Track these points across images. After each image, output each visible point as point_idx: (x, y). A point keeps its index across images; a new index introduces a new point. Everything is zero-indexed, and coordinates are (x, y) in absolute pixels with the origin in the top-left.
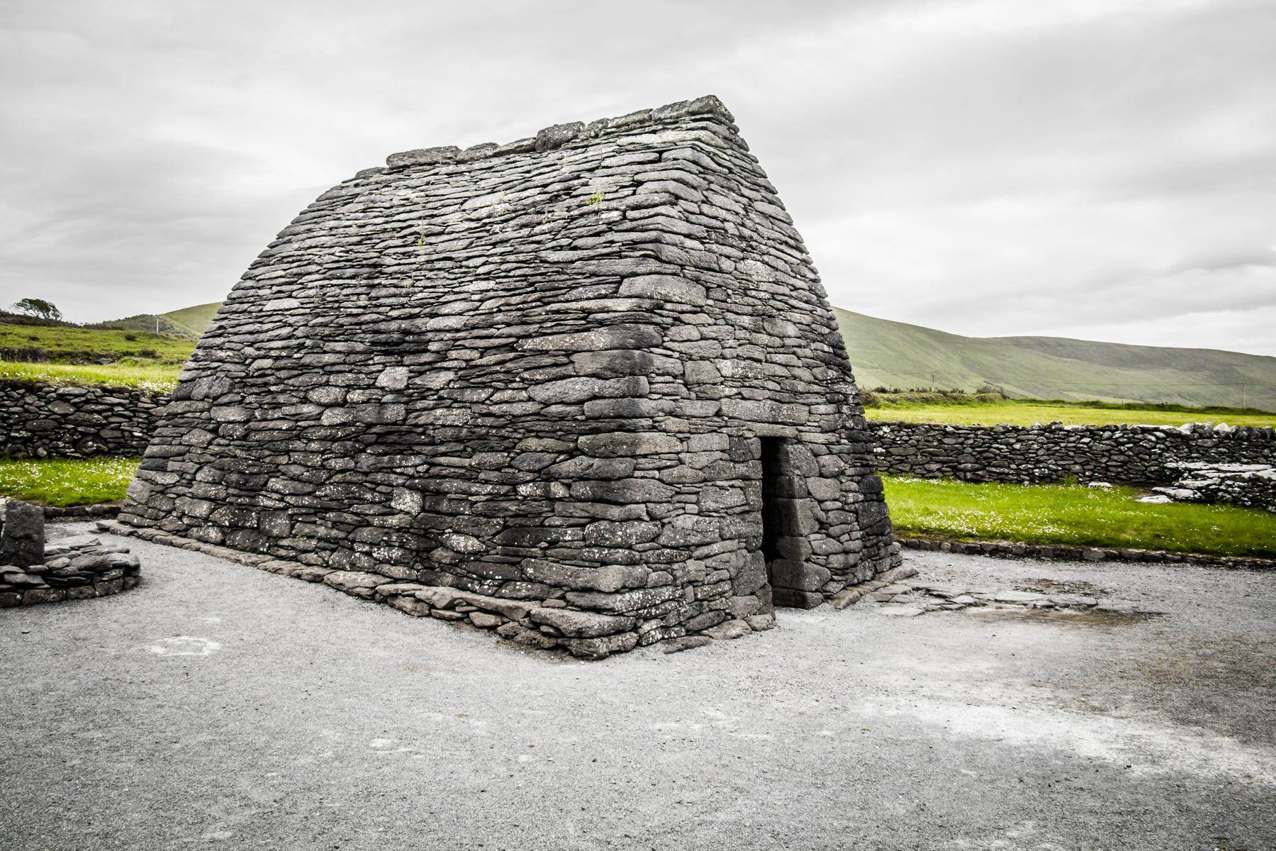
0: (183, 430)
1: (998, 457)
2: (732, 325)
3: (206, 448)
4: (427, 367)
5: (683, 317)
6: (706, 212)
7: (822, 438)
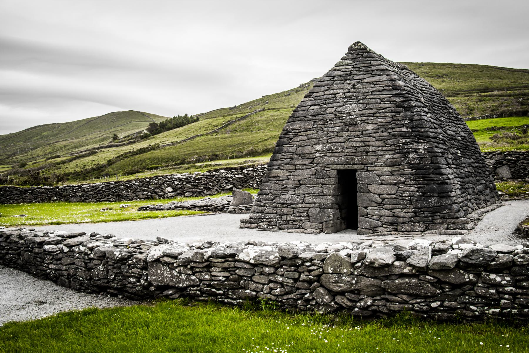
5: (299, 134)
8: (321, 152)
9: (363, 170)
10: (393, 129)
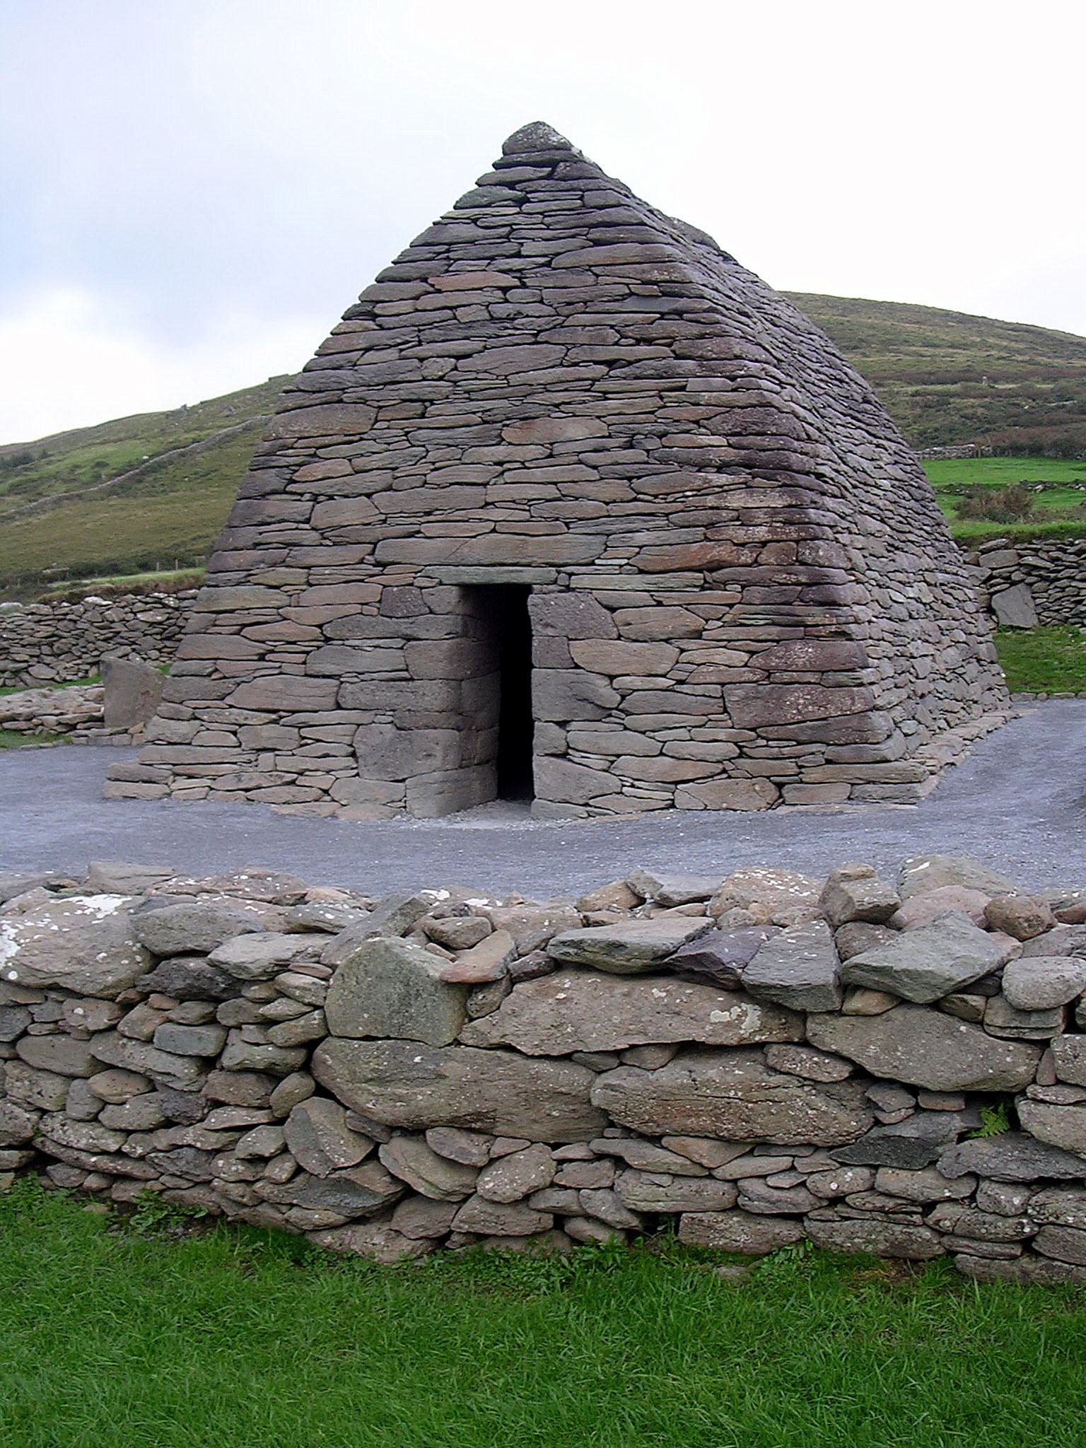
2: (424, 446)
5: (321, 452)
7: (639, 581)
8: (400, 521)
9: (551, 587)
10: (661, 436)
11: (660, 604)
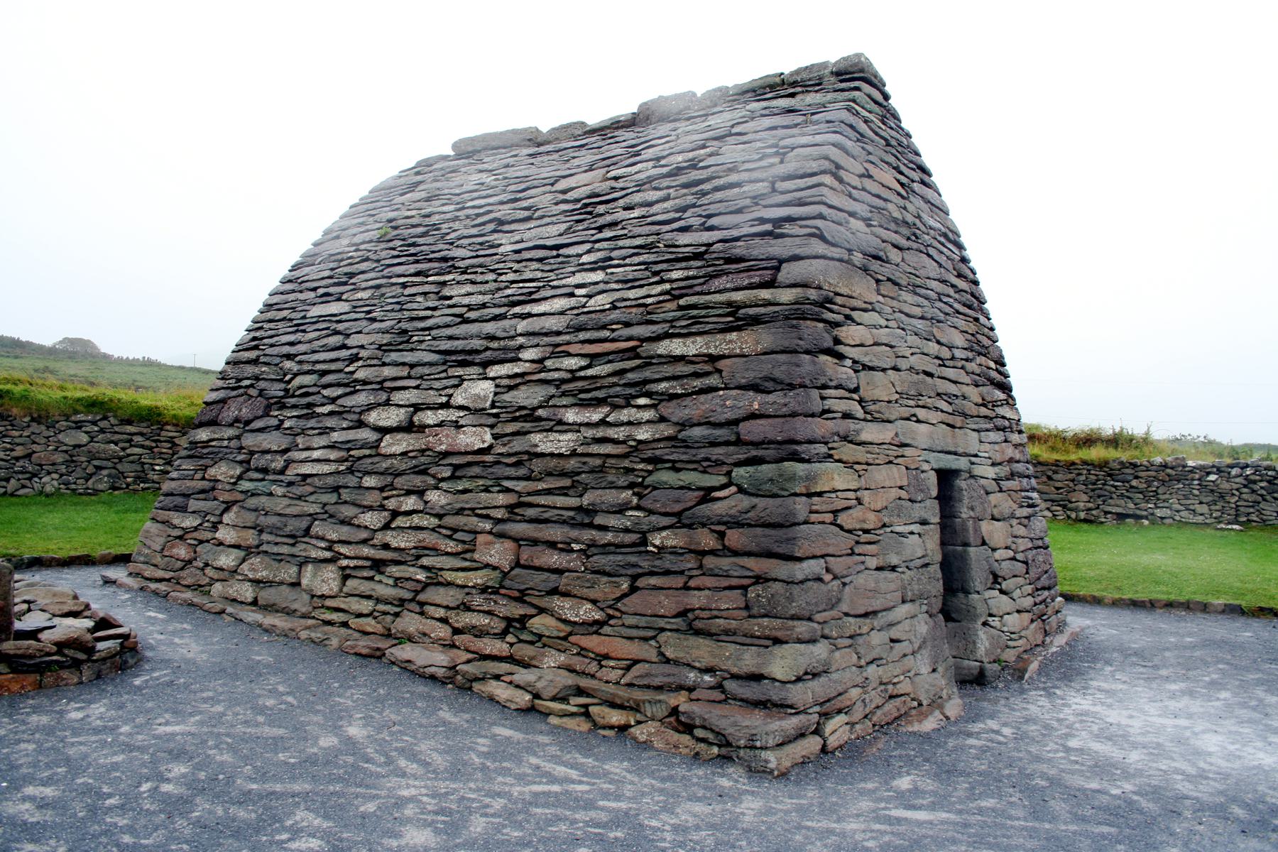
0: (209, 462)
1: (1114, 496)
2: (903, 329)
3: (235, 484)
4: (518, 380)
5: (855, 314)
6: (868, 188)
7: (991, 472)
11: (1001, 491)
